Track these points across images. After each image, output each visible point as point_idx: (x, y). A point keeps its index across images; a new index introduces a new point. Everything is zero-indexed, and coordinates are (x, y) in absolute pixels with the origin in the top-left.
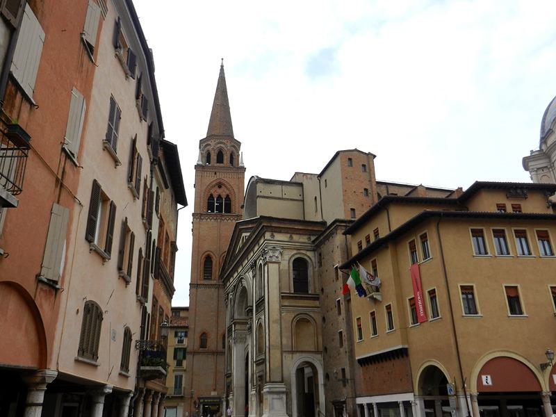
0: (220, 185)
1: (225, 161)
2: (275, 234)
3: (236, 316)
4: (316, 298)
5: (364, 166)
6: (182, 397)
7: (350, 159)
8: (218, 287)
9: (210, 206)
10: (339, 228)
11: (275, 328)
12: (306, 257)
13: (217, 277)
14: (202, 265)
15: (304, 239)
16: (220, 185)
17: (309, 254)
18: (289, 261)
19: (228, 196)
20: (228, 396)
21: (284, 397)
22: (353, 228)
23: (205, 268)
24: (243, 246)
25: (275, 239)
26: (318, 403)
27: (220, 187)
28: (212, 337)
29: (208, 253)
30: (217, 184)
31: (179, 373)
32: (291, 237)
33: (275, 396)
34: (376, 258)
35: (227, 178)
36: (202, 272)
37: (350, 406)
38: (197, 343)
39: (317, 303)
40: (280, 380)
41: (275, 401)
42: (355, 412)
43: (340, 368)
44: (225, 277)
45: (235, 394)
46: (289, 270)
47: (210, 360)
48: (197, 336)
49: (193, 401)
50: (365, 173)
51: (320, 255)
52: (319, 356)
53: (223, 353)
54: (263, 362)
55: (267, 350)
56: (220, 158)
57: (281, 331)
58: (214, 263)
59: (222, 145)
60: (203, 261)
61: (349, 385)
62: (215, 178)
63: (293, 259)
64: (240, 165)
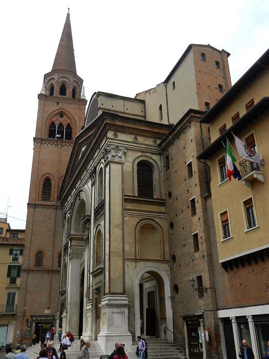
0: (62, 114)
1: (68, 94)
2: (118, 134)
3: (72, 232)
4: (162, 203)
5: (217, 63)
6: (14, 315)
7: (203, 55)
8: (55, 208)
9: (51, 134)
10: (194, 119)
11: (117, 232)
12: (151, 160)
13: (56, 198)
14: (41, 187)
15: (149, 142)
16: (62, 114)
17: (155, 157)
18: (133, 162)
19: (69, 125)
20: (61, 314)
21: (126, 311)
22: (210, 116)
23: (43, 189)
24: (83, 156)
25: (118, 138)
26: (165, 319)
27: (62, 116)
29: (46, 176)
30: (58, 113)
31: (11, 291)
32: (136, 138)
33: (115, 310)
34: (253, 131)
35: (69, 108)
37: (209, 320)
38: (33, 262)
39: (163, 209)
40: (121, 290)
41: (115, 315)
42: (217, 328)
43: (195, 276)
44: (62, 198)
45: (68, 312)
46: (133, 171)
47: (46, 278)
48: (33, 254)
49: (25, 319)
50: (218, 70)
51: (167, 158)
52: (165, 266)
53: (58, 271)
54: (102, 272)
55: (107, 257)
56: (63, 90)
57: (123, 237)
58: (53, 186)
59: (65, 80)
60: (42, 183)
61: (208, 296)
62: (58, 108)
63: (137, 161)
64: (82, 97)
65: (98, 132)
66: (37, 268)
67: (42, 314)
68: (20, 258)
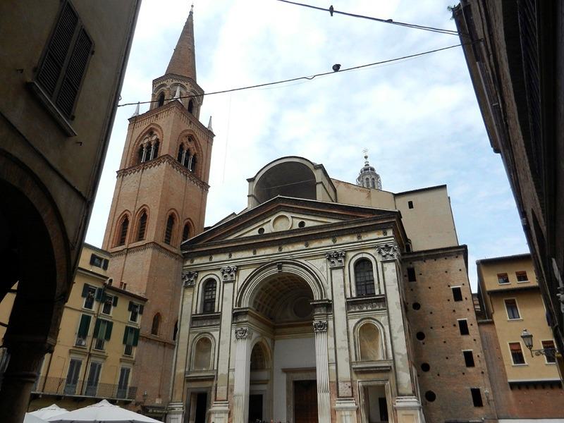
27: (190, 140)
29: (173, 211)
31: (126, 365)
36: (165, 235)
38: (150, 327)
60: (168, 217)
65: (370, 221)
66: (153, 336)
67: (153, 405)
68: (139, 318)
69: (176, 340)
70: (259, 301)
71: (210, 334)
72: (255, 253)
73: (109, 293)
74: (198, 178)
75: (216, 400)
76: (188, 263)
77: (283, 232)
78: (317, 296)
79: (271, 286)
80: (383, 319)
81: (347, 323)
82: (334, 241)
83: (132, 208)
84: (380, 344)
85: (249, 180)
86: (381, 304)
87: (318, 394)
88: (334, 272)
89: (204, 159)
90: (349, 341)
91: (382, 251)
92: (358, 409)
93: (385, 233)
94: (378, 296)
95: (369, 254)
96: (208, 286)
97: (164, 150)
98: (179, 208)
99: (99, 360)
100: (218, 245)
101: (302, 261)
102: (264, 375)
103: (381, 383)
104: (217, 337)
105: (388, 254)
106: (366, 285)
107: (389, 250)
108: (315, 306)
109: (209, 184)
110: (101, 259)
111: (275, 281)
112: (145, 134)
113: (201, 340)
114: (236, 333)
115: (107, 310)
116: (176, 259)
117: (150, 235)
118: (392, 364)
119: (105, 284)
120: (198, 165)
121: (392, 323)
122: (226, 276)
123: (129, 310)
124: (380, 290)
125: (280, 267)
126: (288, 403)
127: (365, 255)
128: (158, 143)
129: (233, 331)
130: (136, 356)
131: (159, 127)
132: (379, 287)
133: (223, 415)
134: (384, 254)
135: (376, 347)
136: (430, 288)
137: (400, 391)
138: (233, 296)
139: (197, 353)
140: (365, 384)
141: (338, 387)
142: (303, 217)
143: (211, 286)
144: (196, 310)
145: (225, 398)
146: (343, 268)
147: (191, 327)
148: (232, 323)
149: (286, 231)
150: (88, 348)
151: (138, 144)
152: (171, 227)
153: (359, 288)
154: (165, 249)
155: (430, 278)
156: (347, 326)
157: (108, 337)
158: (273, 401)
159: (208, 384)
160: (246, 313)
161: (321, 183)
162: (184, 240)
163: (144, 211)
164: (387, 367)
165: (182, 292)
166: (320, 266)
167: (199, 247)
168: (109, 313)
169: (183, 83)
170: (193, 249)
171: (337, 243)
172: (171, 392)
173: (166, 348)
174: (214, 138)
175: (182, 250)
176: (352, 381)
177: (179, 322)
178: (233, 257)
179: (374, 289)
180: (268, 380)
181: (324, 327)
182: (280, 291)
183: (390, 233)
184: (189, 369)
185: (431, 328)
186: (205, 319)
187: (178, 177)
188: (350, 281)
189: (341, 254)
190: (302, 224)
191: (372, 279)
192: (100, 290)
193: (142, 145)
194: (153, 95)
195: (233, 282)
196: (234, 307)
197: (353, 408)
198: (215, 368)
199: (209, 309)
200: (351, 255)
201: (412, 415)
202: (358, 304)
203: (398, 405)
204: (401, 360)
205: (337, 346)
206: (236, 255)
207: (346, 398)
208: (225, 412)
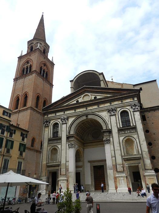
13: (42, 109)
27: (44, 66)
28: (37, 142)
29: (39, 94)
31: (20, 160)
38: (30, 144)
60: (36, 97)
65: (126, 94)
68: (25, 139)
69: (42, 150)
70: (77, 132)
71: (57, 146)
72: (75, 111)
73: (12, 128)
74: (48, 81)
75: (61, 175)
76: (46, 117)
77: (88, 101)
78: (104, 128)
79: (82, 125)
80: (135, 136)
81: (119, 139)
82: (111, 104)
83: (20, 93)
84: (134, 147)
85: (71, 81)
86: (134, 130)
87: (108, 171)
88: (111, 117)
89: (51, 74)
90: (120, 147)
91: (133, 107)
92: (127, 177)
93: (133, 99)
94: (132, 126)
95: (127, 108)
96: (55, 126)
97: (34, 69)
98: (41, 93)
99: (8, 158)
100: (59, 108)
101: (97, 113)
102: (80, 164)
103: (137, 165)
104: (60, 148)
105: (135, 108)
106: (126, 122)
107: (136, 106)
108: (104, 132)
109: (53, 84)
110: (7, 113)
111: (84, 123)
112: (25, 63)
113: (53, 149)
114: (69, 145)
115: (11, 135)
116: (41, 115)
117: (30, 103)
118: (141, 156)
119: (10, 124)
120: (48, 76)
121: (140, 138)
122: (63, 121)
123: (21, 136)
124: (133, 124)
125: (87, 116)
126: (91, 176)
127: (125, 109)
128: (31, 66)
129: (67, 145)
130: (25, 156)
131: (32, 60)
132: (133, 123)
133: (64, 181)
134: (134, 108)
135: (133, 149)
136: (153, 123)
137: (146, 168)
138: (66, 130)
139: (51, 155)
140: (129, 165)
141: (116, 167)
142: (96, 94)
143: (56, 126)
144: (50, 136)
145: (65, 174)
146: (115, 115)
147: (48, 144)
148: (66, 141)
149: (89, 101)
150: (3, 153)
151: (23, 67)
152: (38, 102)
153: (123, 123)
154: (36, 110)
155: (153, 119)
156: (119, 140)
157: (12, 147)
158: (85, 175)
159: (57, 168)
160: (73, 136)
161: (103, 80)
162: (43, 107)
163: (26, 94)
164: (139, 157)
165: (44, 129)
166: (105, 115)
167: (50, 110)
168: (12, 137)
169: (40, 42)
170: (48, 110)
171: (112, 104)
172: (40, 172)
173: (38, 153)
174: (55, 66)
175: (43, 111)
176: (123, 164)
177: (43, 142)
178: (66, 113)
179: (130, 123)
180: (82, 166)
181: (108, 141)
182: (86, 128)
183: (136, 99)
184: (48, 161)
185: (155, 140)
186: (54, 140)
187: (40, 80)
188: (119, 121)
189: (114, 109)
190: (95, 98)
191: (128, 119)
192: (7, 126)
193: (24, 68)
194: (28, 48)
195: (66, 123)
196: (67, 134)
197: (124, 176)
198: (60, 161)
199: (56, 136)
200: (118, 109)
201: (153, 178)
202: (123, 130)
203: (145, 174)
204: (145, 154)
205: (115, 149)
206: (67, 112)
207: (120, 172)
208: (65, 180)
